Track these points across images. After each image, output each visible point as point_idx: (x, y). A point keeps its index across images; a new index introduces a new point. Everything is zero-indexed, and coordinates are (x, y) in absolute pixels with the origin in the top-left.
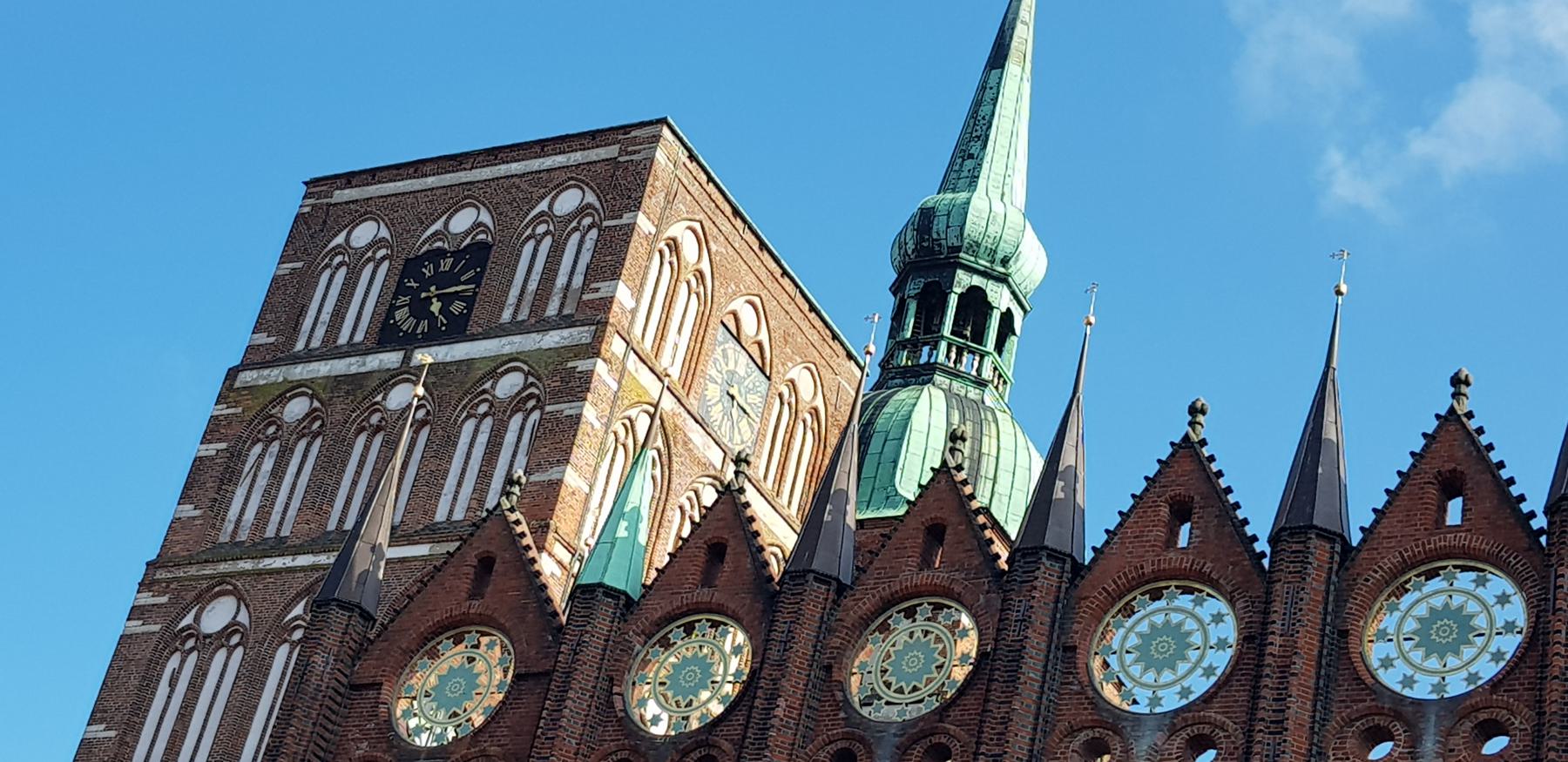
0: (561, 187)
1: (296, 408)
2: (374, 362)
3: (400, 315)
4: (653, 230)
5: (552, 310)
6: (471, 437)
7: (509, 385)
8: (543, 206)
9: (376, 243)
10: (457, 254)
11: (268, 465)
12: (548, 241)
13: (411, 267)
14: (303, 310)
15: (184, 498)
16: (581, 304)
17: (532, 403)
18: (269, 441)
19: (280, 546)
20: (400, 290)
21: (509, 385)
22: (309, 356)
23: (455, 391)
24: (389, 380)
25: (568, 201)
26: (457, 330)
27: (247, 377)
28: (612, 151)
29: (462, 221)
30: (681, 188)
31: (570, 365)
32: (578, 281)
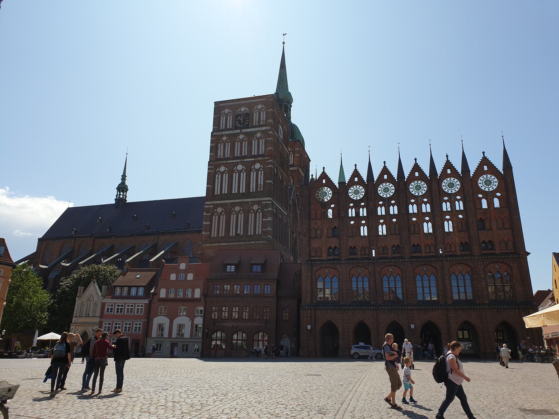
1: (225, 138)
2: (236, 131)
3: (237, 124)
5: (261, 123)
7: (259, 135)
9: (229, 113)
10: (244, 115)
11: (222, 147)
13: (236, 117)
14: (220, 123)
15: (210, 152)
18: (221, 143)
19: (228, 159)
20: (236, 120)
21: (259, 135)
22: (223, 130)
23: (250, 136)
24: (239, 134)
25: (260, 107)
26: (248, 127)
27: (215, 133)
28: (265, 99)
29: (243, 109)
32: (264, 119)
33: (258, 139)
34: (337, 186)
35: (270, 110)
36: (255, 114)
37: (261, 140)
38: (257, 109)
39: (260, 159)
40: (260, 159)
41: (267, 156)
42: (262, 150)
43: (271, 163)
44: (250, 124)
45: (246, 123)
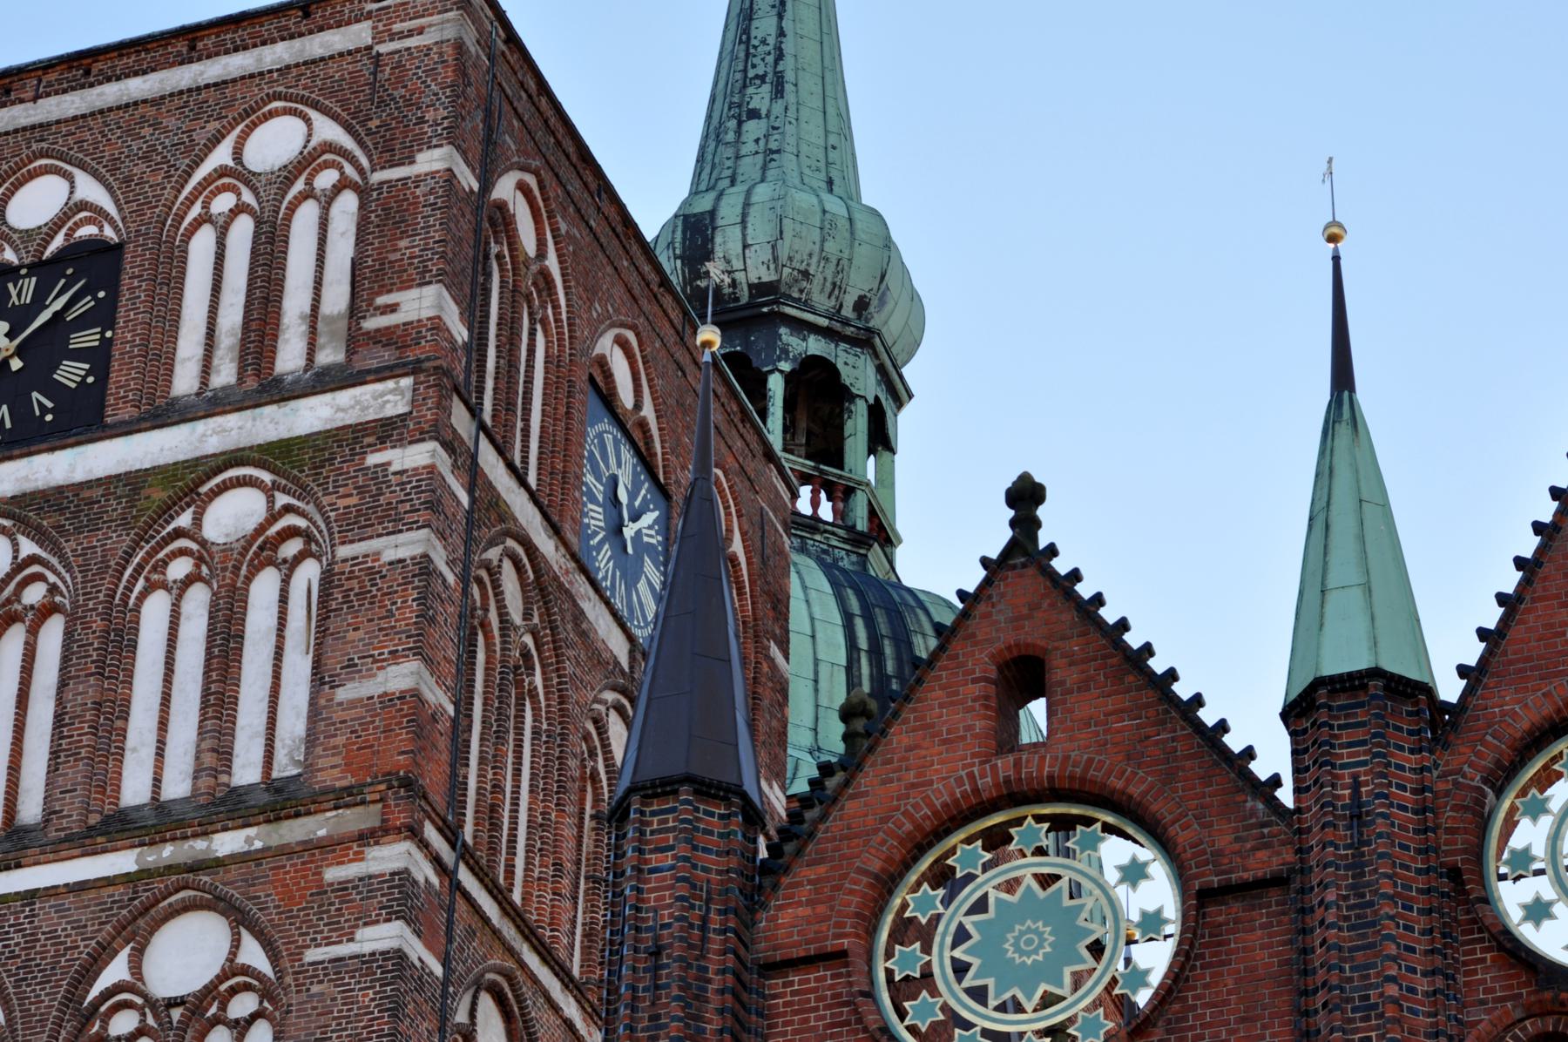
0: (254, 116)
4: (476, 186)
5: (290, 357)
6: (168, 631)
7: (233, 514)
8: (222, 156)
12: (243, 229)
16: (356, 340)
17: (291, 548)
21: (233, 514)
25: (275, 142)
26: (83, 419)
29: (36, 203)
30: (506, 107)
31: (373, 459)
32: (337, 298)
33: (227, 576)
34: (1273, 757)
35: (431, 161)
36: (202, 245)
37: (264, 587)
38: (238, 174)
39: (228, 843)
40: (228, 843)
41: (343, 798)
42: (274, 724)
43: (398, 898)
44: (122, 378)
45: (70, 373)
